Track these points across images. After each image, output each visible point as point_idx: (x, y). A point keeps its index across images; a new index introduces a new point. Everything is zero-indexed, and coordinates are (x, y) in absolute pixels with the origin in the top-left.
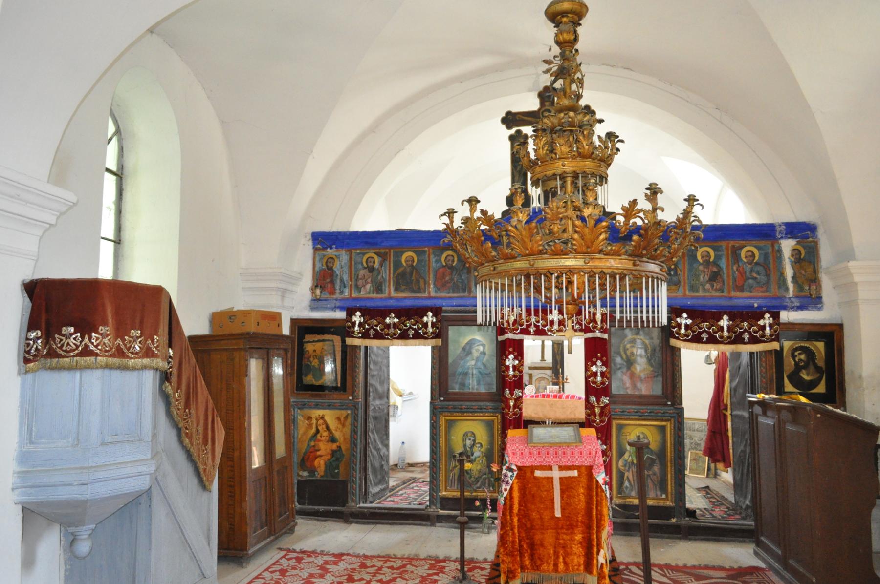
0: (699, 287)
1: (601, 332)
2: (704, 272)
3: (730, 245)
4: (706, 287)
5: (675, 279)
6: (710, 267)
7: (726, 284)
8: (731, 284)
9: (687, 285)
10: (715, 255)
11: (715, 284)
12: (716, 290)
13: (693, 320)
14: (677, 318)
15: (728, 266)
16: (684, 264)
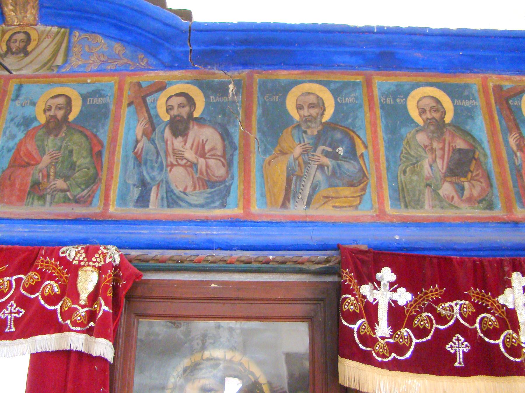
0: (421, 193)
1: (90, 332)
2: (433, 150)
3: (491, 84)
4: (441, 192)
5: (350, 167)
6: (448, 138)
7: (495, 182)
8: (510, 184)
9: (385, 185)
10: (455, 107)
11: (466, 185)
12: (470, 200)
13: (415, 294)
14: (361, 283)
15: (493, 133)
16: (374, 125)
